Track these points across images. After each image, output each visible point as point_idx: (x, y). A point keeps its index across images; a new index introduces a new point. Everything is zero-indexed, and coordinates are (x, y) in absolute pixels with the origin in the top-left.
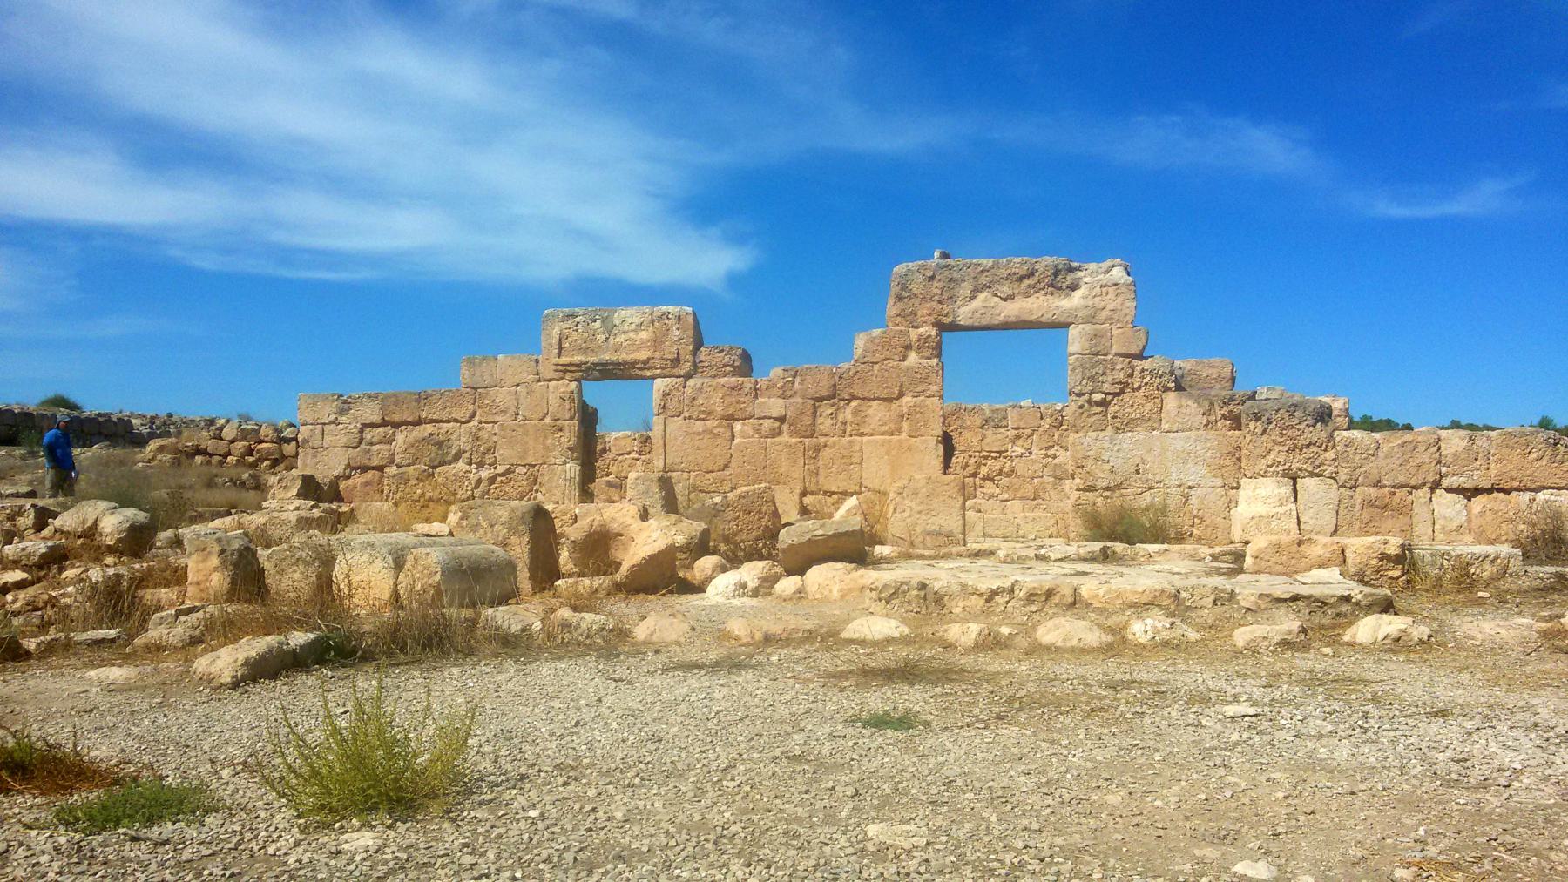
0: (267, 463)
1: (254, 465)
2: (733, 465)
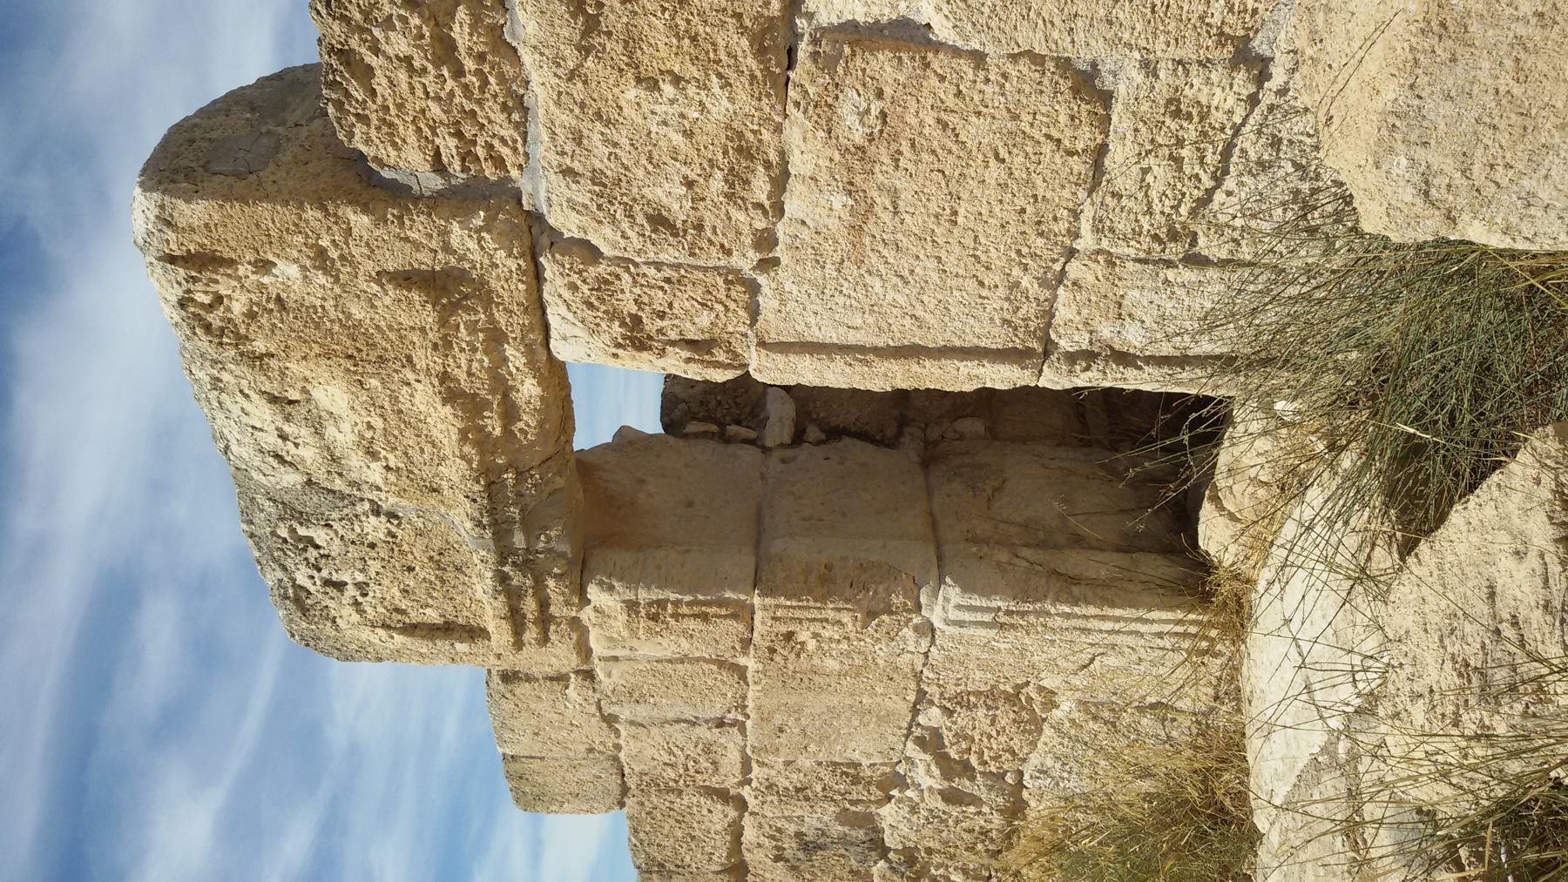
2: (1087, 48)
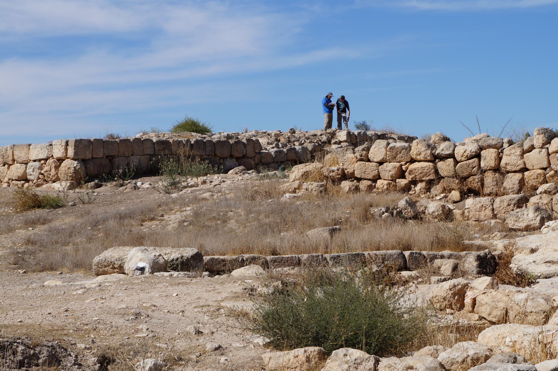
0: (420, 186)
1: (406, 189)
